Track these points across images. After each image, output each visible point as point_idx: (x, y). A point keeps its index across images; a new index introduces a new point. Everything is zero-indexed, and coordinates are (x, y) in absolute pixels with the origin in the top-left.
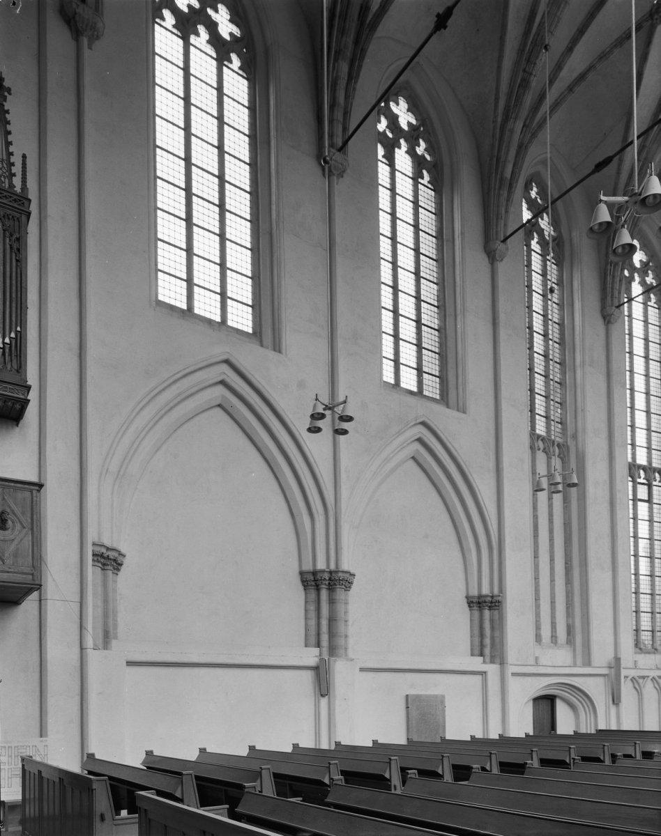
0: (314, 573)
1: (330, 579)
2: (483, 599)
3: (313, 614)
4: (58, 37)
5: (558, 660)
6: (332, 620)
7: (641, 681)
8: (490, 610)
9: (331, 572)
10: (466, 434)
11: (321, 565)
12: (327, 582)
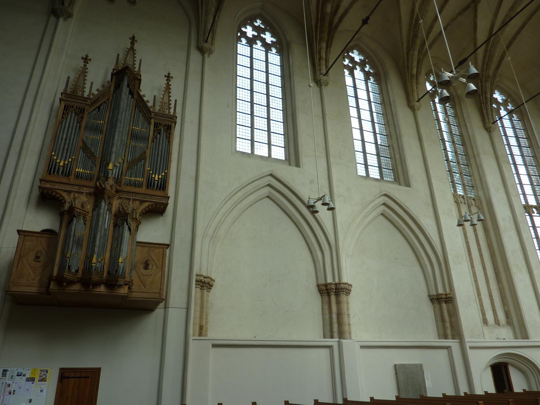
0: (326, 285)
1: (336, 289)
3: (327, 311)
4: (195, 55)
6: (339, 314)
9: (336, 284)
10: (414, 200)
11: (330, 280)
12: (334, 291)
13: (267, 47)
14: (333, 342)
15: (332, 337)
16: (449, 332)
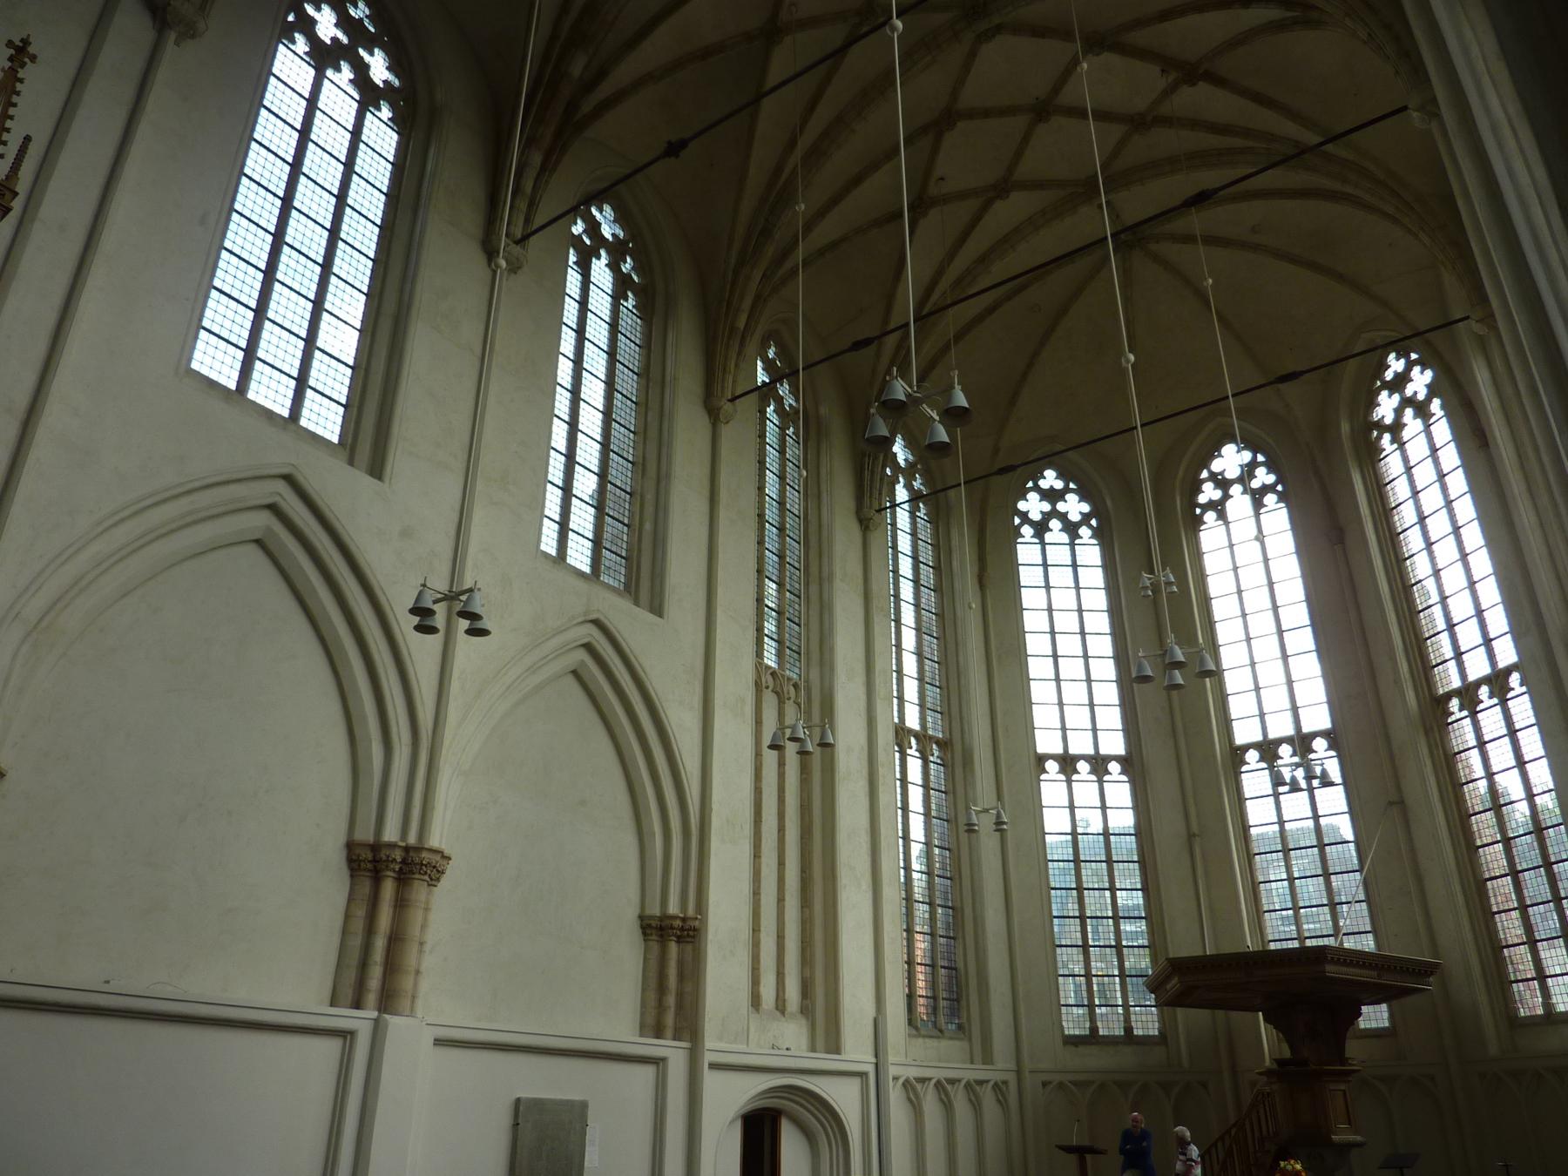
0: (376, 847)
1: (404, 861)
2: (668, 922)
3: (358, 925)
5: (787, 1041)
6: (396, 939)
7: (919, 1086)
8: (678, 942)
9: (407, 849)
10: (662, 650)
11: (391, 834)
12: (397, 868)
13: (369, 95)
14: (360, 1021)
15: (357, 1004)
16: (670, 1019)
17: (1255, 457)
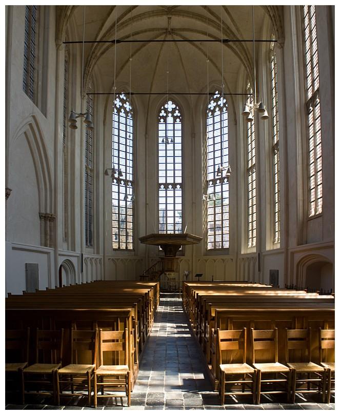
17: (176, 107)
